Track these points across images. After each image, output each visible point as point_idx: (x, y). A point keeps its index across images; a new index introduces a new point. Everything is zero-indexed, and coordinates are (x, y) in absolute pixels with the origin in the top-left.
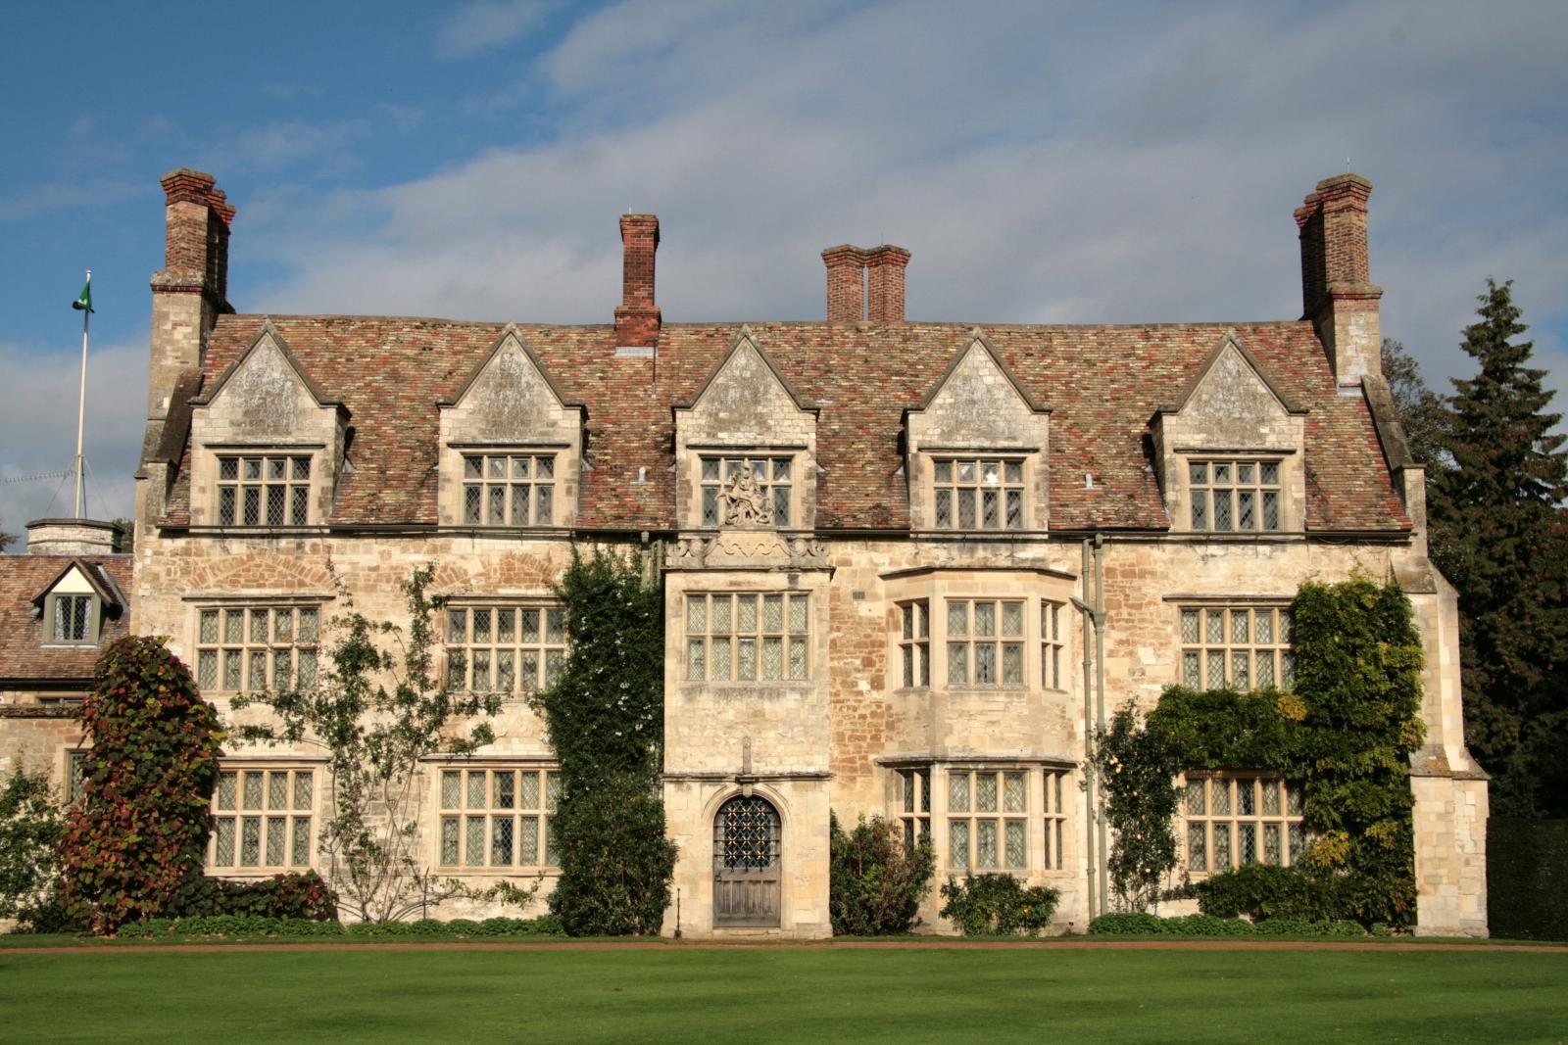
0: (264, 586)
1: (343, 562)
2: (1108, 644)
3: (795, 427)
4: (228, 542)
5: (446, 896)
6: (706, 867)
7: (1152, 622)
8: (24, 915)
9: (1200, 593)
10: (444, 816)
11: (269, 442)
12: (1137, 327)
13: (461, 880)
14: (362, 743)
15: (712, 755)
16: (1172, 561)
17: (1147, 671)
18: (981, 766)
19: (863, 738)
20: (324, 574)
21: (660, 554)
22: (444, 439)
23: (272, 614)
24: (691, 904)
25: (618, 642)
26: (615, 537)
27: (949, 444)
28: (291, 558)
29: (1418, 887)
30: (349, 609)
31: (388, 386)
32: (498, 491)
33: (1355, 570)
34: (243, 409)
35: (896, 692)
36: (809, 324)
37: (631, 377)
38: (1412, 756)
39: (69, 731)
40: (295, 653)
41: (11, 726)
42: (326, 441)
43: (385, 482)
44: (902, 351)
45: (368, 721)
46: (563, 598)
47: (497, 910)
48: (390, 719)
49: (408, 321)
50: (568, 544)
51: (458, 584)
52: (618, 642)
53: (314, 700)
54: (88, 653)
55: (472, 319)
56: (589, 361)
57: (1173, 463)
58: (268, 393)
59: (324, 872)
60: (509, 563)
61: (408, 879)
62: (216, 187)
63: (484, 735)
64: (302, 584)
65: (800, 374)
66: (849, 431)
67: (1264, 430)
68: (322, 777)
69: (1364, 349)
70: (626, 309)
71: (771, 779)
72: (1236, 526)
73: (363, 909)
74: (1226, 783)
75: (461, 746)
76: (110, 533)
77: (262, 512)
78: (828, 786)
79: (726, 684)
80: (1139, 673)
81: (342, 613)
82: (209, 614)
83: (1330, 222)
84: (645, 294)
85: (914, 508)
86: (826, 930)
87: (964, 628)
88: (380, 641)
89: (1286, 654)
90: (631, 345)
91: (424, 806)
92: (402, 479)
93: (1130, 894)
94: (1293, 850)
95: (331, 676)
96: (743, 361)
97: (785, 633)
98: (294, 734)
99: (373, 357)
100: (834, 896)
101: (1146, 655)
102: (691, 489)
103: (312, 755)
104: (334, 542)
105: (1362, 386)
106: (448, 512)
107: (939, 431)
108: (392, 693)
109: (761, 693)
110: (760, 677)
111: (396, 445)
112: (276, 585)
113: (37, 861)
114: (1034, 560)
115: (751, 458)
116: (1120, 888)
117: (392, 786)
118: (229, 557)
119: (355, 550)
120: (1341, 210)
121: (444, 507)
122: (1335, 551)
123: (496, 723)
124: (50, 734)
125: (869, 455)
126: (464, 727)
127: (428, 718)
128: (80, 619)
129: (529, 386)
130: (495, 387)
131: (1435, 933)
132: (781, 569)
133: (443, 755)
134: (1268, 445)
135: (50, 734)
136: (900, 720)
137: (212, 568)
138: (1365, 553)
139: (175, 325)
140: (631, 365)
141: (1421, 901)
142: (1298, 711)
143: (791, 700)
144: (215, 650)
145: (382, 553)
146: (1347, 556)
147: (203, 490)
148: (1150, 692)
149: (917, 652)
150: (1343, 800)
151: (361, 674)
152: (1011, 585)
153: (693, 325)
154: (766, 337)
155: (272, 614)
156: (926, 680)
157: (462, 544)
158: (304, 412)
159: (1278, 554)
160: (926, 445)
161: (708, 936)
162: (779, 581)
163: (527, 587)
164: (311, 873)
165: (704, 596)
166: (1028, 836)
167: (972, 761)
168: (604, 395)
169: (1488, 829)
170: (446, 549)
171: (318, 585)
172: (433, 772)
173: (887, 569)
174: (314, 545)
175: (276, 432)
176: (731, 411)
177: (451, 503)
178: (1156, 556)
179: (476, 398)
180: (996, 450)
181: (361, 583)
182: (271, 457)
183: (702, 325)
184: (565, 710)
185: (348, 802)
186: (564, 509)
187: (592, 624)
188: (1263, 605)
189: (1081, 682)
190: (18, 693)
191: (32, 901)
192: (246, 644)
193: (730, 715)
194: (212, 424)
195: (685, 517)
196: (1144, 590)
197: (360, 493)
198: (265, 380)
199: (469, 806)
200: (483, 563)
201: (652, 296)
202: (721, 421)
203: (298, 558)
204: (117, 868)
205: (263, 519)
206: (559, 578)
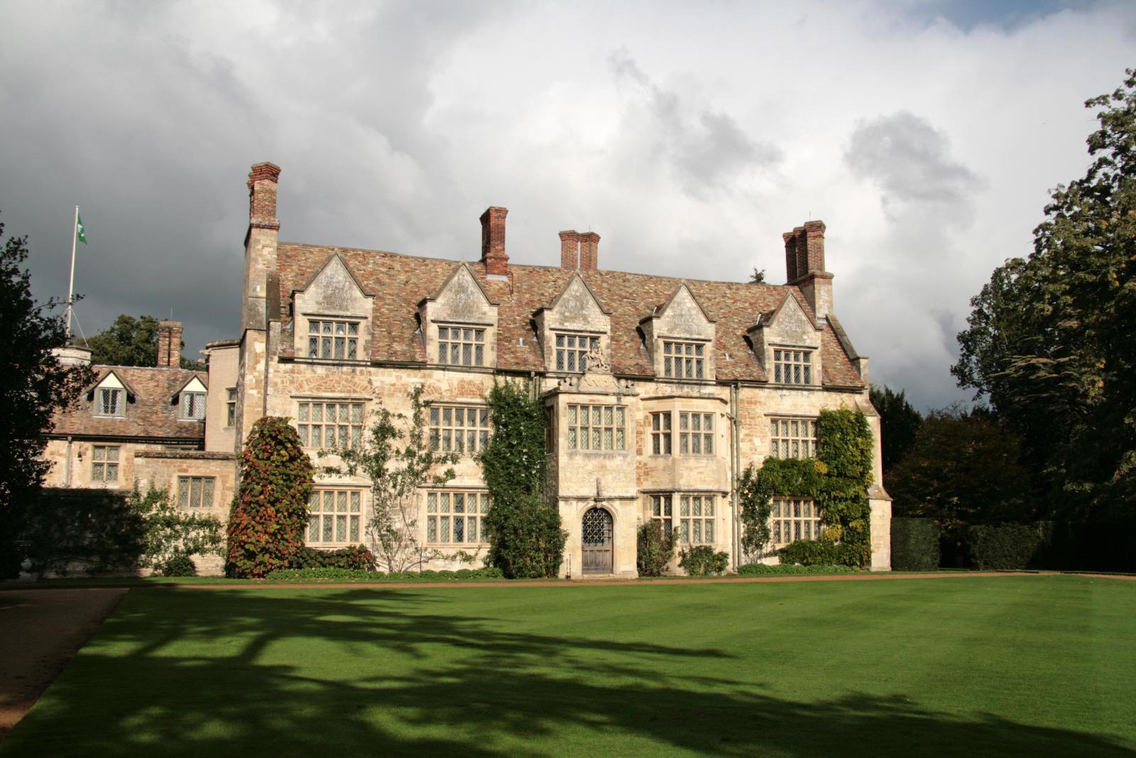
0: (334, 391)
1: (376, 381)
2: (741, 436)
3: (601, 323)
4: (315, 367)
5: (431, 558)
8: (157, 567)
9: (780, 412)
10: (429, 517)
11: (337, 314)
12: (724, 283)
14: (387, 477)
15: (581, 487)
16: (768, 397)
17: (758, 449)
18: (696, 494)
21: (538, 383)
23: (338, 407)
24: (572, 561)
26: (515, 373)
27: (671, 335)
28: (349, 377)
29: (872, 548)
30: (380, 406)
31: (377, 287)
32: (455, 346)
33: (841, 404)
34: (323, 295)
35: (650, 457)
38: (869, 490)
39: (179, 466)
40: (350, 428)
41: (147, 462)
42: (368, 315)
43: (393, 339)
44: (625, 286)
45: (391, 466)
46: (491, 405)
47: (456, 567)
48: (404, 465)
49: (378, 253)
50: (492, 376)
52: (522, 428)
53: (362, 454)
57: (768, 351)
59: (368, 546)
60: (462, 385)
61: (412, 549)
63: (451, 474)
64: (355, 391)
67: (805, 337)
68: (367, 496)
69: (827, 301)
71: (610, 499)
73: (389, 564)
74: (789, 502)
76: (90, 354)
78: (637, 504)
79: (588, 451)
81: (377, 408)
82: (302, 405)
83: (810, 242)
84: (501, 248)
85: (656, 366)
86: (635, 574)
87: (686, 427)
88: (396, 423)
89: (813, 442)
91: (420, 509)
93: (751, 555)
94: (815, 533)
95: (371, 441)
96: (576, 287)
97: (615, 426)
98: (352, 472)
100: (639, 558)
101: (757, 441)
106: (431, 357)
108: (403, 451)
109: (605, 456)
111: (391, 319)
112: (341, 392)
113: (164, 537)
114: (709, 394)
115: (580, 337)
116: (746, 553)
117: (404, 500)
119: (383, 374)
120: (816, 237)
122: (833, 395)
123: (456, 468)
124: (169, 467)
125: (625, 338)
126: (440, 470)
127: (422, 465)
128: (114, 402)
129: (472, 293)
131: (879, 570)
132: (614, 394)
133: (430, 485)
134: (807, 345)
135: (169, 467)
136: (652, 471)
137: (307, 381)
138: (845, 396)
139: (264, 247)
141: (873, 556)
142: (824, 469)
143: (618, 461)
144: (307, 425)
145: (397, 377)
147: (301, 338)
150: (843, 510)
151: (387, 441)
152: (708, 406)
153: (521, 266)
154: (558, 274)
155: (338, 407)
157: (438, 374)
158: (355, 299)
159: (811, 395)
161: (581, 578)
162: (612, 400)
163: (472, 398)
164: (362, 546)
166: (715, 527)
167: (693, 491)
169: (891, 523)
170: (430, 376)
172: (424, 492)
174: (362, 373)
175: (341, 309)
177: (433, 352)
178: (761, 394)
180: (693, 340)
182: (338, 322)
184: (492, 462)
185: (381, 509)
186: (490, 358)
187: (507, 419)
188: (804, 419)
189: (730, 454)
190: (82, 443)
191: (161, 558)
192: (325, 422)
193: (590, 467)
194: (306, 303)
195: (549, 365)
196: (757, 410)
197: (381, 344)
201: (504, 249)
202: (565, 317)
204: (267, 542)
206: (487, 393)
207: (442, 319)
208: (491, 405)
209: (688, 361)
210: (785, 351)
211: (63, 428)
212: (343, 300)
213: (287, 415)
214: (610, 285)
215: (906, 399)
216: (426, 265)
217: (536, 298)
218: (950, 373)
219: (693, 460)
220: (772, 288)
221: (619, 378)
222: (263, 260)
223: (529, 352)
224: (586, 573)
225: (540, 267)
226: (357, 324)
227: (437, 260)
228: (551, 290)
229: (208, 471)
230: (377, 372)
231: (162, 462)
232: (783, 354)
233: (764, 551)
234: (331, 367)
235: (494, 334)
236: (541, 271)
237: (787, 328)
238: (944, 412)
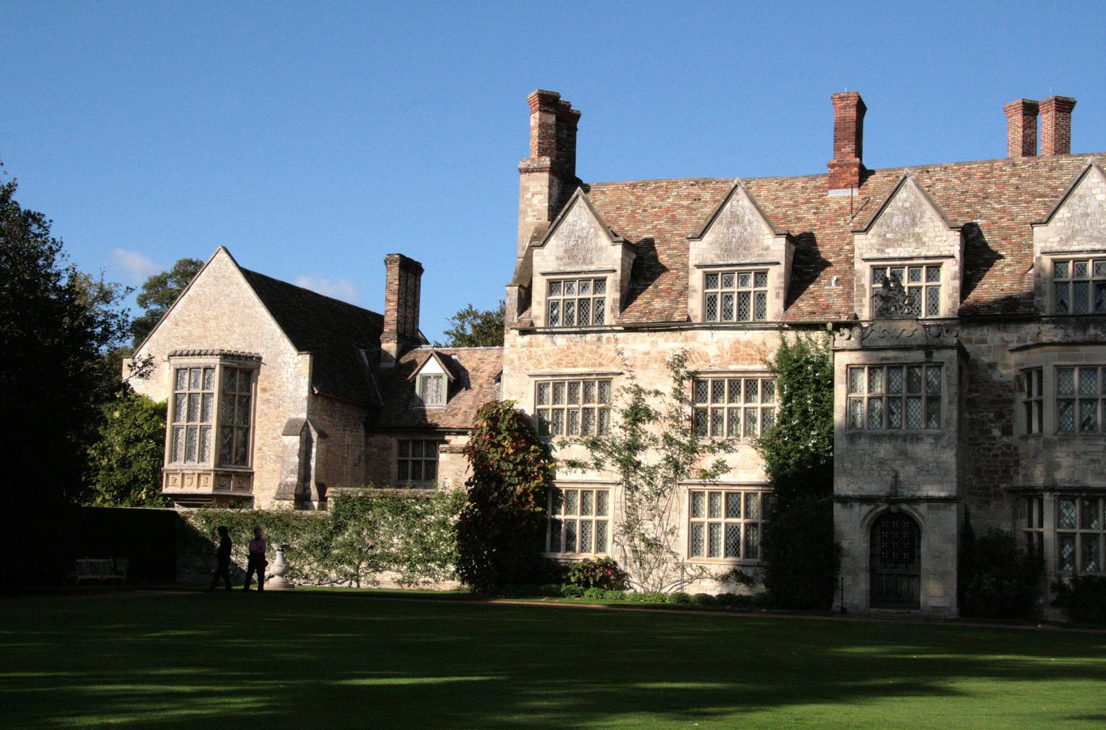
6: (864, 563)
11: (580, 269)
13: (706, 566)
19: (996, 472)
20: (614, 358)
22: (693, 261)
24: (855, 589)
25: (809, 402)
27: (1066, 248)
30: (630, 381)
34: (564, 248)
35: (1021, 438)
36: (976, 163)
37: (836, 211)
41: (452, 459)
50: (777, 333)
51: (702, 363)
52: (809, 402)
56: (808, 201)
58: (579, 237)
59: (617, 558)
61: (671, 565)
62: (561, 99)
63: (721, 467)
64: (601, 365)
65: (964, 201)
66: (995, 242)
68: (616, 497)
70: (835, 162)
75: (705, 474)
77: (581, 319)
78: (954, 507)
88: (652, 402)
90: (839, 188)
92: (668, 292)
98: (599, 465)
99: (660, 208)
102: (865, 290)
103: (608, 480)
107: (1057, 239)
110: (904, 427)
112: (584, 366)
115: (910, 266)
117: (662, 503)
118: (556, 347)
121: (692, 310)
123: (730, 459)
126: (707, 461)
129: (750, 223)
132: (919, 347)
137: (545, 355)
139: (534, 194)
140: (838, 203)
145: (652, 343)
147: (539, 303)
149: (1035, 408)
153: (887, 170)
154: (941, 175)
156: (1041, 429)
158: (601, 248)
160: (1047, 250)
162: (919, 356)
163: (751, 364)
164: (608, 558)
165: (902, 367)
168: (815, 225)
170: (694, 339)
173: (1013, 345)
174: (608, 338)
175: (584, 262)
176: (896, 233)
177: (695, 306)
179: (714, 233)
181: (638, 364)
195: (861, 311)
198: (577, 228)
200: (718, 347)
203: (598, 347)
206: (771, 357)
207: (709, 263)
208: (773, 371)
211: (466, 422)
219: (1078, 442)
222: (533, 211)
223: (839, 295)
226: (604, 279)
230: (627, 339)
234: (573, 335)
235: (779, 274)
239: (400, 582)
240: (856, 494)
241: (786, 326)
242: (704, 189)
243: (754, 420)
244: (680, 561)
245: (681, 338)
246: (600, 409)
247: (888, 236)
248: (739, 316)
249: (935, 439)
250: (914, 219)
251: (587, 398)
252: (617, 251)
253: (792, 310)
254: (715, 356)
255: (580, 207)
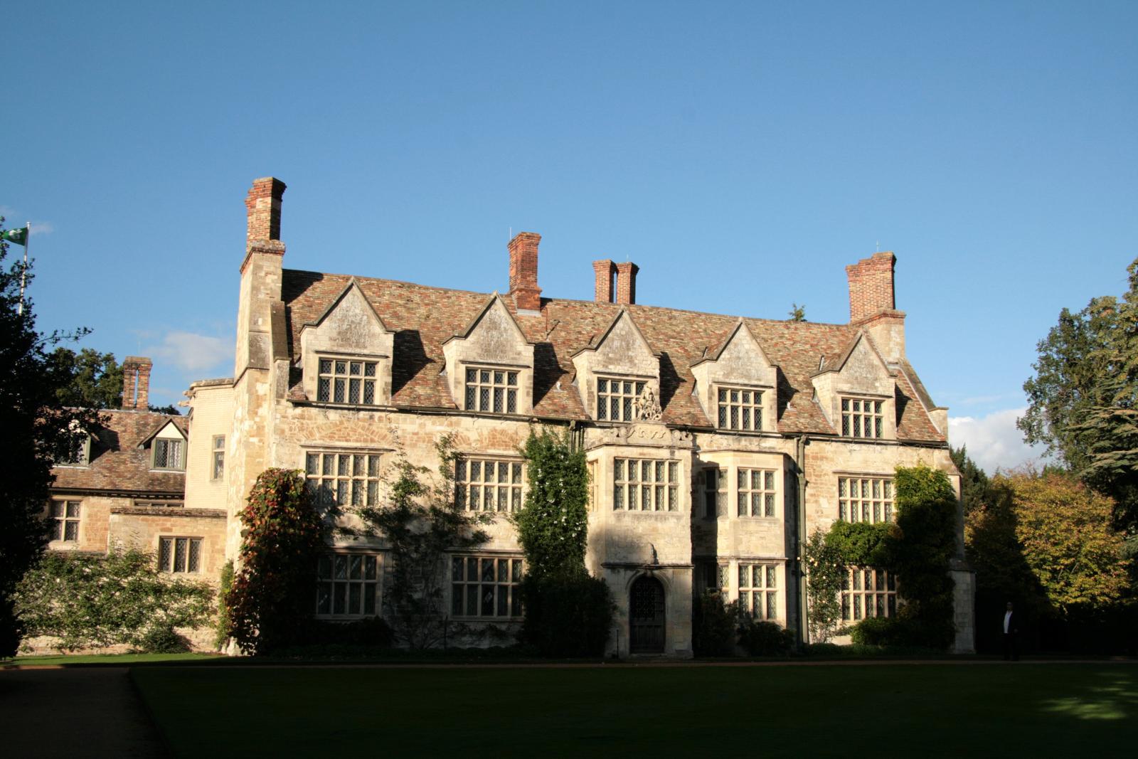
7: (826, 485)
9: (849, 470)
11: (353, 352)
13: (466, 624)
16: (835, 452)
18: (757, 562)
20: (386, 436)
24: (621, 641)
27: (727, 381)
28: (366, 425)
39: (163, 524)
41: (125, 520)
42: (388, 355)
44: (671, 324)
46: (526, 457)
47: (485, 644)
49: (394, 282)
50: (527, 424)
51: (464, 445)
54: (83, 472)
55: (429, 285)
58: (352, 322)
59: (386, 618)
61: (435, 623)
64: (372, 441)
67: (877, 384)
69: (898, 344)
70: (522, 287)
72: (862, 434)
80: (820, 512)
81: (398, 460)
84: (533, 279)
88: (421, 478)
90: (525, 308)
104: (392, 415)
105: (897, 363)
107: (722, 373)
112: (357, 441)
114: (769, 448)
118: (328, 422)
121: (457, 399)
122: (909, 450)
130: (487, 329)
134: (879, 393)
137: (318, 428)
139: (267, 274)
141: (957, 636)
143: (672, 522)
146: (915, 453)
147: (312, 379)
148: (826, 523)
154: (596, 310)
157: (466, 421)
158: (374, 335)
159: (884, 451)
162: (664, 454)
163: (505, 450)
164: (377, 617)
167: (754, 559)
170: (458, 424)
171: (383, 442)
174: (380, 419)
175: (357, 346)
177: (459, 396)
178: (829, 448)
181: (408, 442)
183: (560, 300)
189: (793, 516)
195: (591, 412)
196: (823, 467)
198: (351, 313)
199: (469, 580)
201: (536, 281)
202: (610, 359)
205: (347, 400)
206: (523, 445)
207: (472, 360)
209: (746, 411)
210: (854, 400)
212: (360, 336)
213: (295, 468)
214: (655, 322)
215: (967, 455)
216: (449, 297)
217: (573, 337)
218: (1015, 426)
220: (835, 328)
221: (673, 427)
222: (266, 289)
224: (635, 653)
225: (576, 302)
226: (376, 363)
227: (460, 291)
228: (589, 328)
229: (195, 530)
230: (398, 419)
231: (142, 520)
232: (851, 404)
233: (832, 629)
234: (346, 412)
236: (578, 306)
237: (858, 374)
238: (1017, 470)
239: (60, 647)
240: (622, 561)
241: (535, 419)
242: (412, 292)
243: (505, 496)
244: (444, 618)
245: (446, 423)
246: (369, 482)
247: (610, 355)
248: (481, 407)
249: (677, 519)
250: (628, 345)
251: (356, 471)
252: (389, 341)
253: (538, 407)
254: (475, 441)
255: (354, 295)
